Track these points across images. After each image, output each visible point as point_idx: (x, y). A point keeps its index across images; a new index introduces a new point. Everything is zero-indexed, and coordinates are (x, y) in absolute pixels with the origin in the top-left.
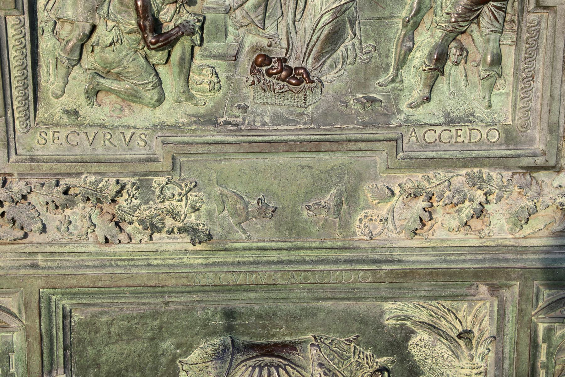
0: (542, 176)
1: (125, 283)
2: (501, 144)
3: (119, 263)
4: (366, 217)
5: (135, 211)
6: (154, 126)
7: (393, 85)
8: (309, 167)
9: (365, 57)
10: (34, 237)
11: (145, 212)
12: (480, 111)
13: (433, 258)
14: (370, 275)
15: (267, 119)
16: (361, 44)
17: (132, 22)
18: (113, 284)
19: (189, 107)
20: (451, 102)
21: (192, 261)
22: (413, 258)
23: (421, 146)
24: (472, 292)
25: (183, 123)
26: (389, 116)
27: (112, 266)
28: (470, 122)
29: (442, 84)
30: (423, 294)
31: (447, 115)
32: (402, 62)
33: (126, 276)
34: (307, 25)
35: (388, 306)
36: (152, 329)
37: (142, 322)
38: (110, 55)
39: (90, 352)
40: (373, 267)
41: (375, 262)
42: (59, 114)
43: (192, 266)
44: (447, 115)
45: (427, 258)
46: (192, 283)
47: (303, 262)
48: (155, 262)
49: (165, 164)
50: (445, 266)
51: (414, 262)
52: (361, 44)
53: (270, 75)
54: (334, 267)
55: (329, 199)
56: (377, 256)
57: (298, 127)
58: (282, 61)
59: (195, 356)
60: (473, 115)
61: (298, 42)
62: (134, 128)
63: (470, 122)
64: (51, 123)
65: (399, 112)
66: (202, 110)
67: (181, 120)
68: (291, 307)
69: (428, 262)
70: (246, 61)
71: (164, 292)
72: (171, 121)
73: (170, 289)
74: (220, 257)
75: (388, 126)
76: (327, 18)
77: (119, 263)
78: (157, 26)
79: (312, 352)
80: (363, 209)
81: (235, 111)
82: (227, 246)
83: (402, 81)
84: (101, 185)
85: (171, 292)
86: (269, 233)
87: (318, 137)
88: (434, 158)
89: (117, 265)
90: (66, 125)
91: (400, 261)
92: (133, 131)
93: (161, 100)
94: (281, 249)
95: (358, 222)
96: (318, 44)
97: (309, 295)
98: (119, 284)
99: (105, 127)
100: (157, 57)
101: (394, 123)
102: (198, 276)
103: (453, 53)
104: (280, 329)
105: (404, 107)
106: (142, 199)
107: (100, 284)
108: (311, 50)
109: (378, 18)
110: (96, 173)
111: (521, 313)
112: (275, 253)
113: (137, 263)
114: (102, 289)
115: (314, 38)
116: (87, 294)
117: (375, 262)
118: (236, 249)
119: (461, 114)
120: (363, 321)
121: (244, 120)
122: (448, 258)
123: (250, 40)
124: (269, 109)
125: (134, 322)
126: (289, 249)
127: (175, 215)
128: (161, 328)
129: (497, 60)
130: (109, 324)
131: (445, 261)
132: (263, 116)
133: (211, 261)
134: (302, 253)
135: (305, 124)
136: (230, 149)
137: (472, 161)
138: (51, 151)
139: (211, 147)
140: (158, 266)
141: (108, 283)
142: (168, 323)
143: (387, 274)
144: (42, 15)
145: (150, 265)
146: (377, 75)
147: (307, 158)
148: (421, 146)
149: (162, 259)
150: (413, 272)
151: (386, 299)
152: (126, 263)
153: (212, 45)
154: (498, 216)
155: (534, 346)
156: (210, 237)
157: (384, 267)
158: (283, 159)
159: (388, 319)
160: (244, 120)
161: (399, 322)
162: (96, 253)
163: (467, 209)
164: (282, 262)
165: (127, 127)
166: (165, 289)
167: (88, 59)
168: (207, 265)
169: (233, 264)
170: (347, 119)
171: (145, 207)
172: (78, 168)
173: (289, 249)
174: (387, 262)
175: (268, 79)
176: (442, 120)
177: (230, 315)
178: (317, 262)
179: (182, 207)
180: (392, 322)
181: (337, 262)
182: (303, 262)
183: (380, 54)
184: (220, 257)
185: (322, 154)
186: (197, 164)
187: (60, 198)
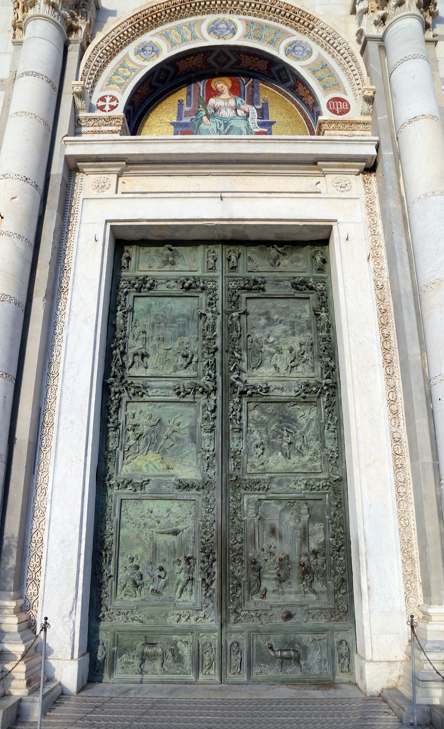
0: (199, 612)
10: (114, 621)
11: (132, 616)
12: (189, 600)
17: (131, 583)
19: (140, 598)
26: (173, 600)
29: (183, 595)
32: (176, 591)
34: (160, 584)
35: (173, 636)
38: (128, 588)
39: (121, 643)
49: (136, 608)
55: (163, 615)
58: (156, 590)
59: (139, 645)
61: (159, 588)
64: (118, 600)
68: (157, 636)
70: (150, 590)
74: (144, 625)
78: (136, 583)
79: (159, 645)
86: (153, 621)
93: (136, 596)
100: (136, 589)
103: (184, 589)
111: (196, 638)
120: (169, 639)
123: (151, 587)
127: (137, 617)
129: (192, 591)
138: (118, 605)
144: (119, 582)
147: (159, 607)
153: (145, 587)
155: (199, 644)
156: (142, 622)
158: (155, 608)
163: (186, 617)
167: (125, 589)
170: (166, 600)
172: (121, 608)
177: (146, 637)
179: (138, 616)
184: (144, 625)
187: (118, 613)
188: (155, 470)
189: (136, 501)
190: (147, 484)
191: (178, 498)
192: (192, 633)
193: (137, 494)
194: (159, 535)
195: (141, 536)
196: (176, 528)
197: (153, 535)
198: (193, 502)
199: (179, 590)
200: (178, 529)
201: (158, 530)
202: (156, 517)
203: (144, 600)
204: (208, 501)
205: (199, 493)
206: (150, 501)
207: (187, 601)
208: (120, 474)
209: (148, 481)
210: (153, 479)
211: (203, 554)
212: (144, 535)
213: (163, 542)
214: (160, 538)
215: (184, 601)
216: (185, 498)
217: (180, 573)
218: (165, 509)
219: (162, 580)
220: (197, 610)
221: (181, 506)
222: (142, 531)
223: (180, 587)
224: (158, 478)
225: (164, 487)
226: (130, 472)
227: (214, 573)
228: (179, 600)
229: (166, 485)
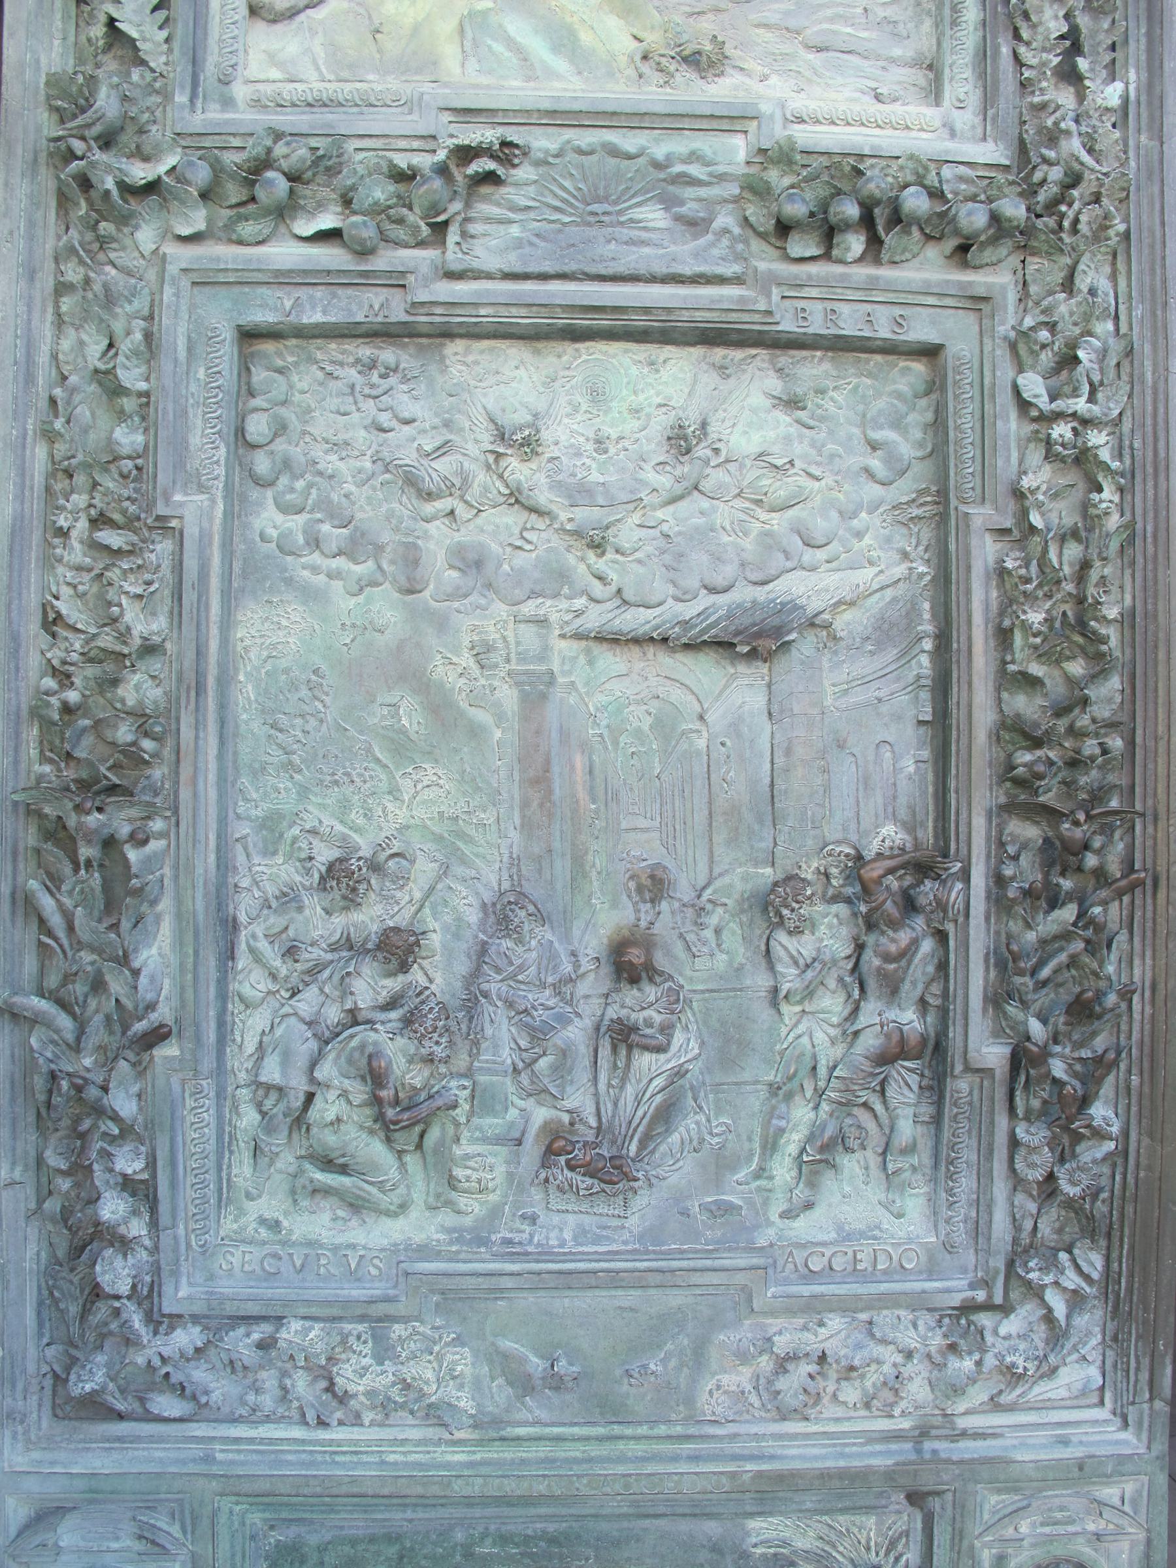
0: (985, 1320)
1: (344, 1489)
2: (921, 1272)
3: (338, 1458)
4: (719, 1387)
5: (362, 1376)
6: (396, 1245)
7: (758, 1183)
8: (632, 1310)
9: (717, 1140)
13: (824, 1451)
14: (724, 1480)
15: (567, 1235)
16: (709, 1121)
18: (327, 1492)
20: (846, 1208)
21: (449, 1457)
22: (794, 1452)
23: (804, 1277)
24: (883, 1502)
25: (438, 1241)
27: (325, 1462)
28: (875, 1238)
30: (809, 1505)
31: (840, 1228)
32: (770, 1145)
33: (347, 1480)
35: (754, 1524)
36: (388, 1559)
37: (373, 1548)
40: (731, 1468)
41: (735, 1458)
42: (254, 1225)
43: (448, 1466)
44: (840, 1228)
45: (815, 1451)
46: (448, 1493)
47: (622, 1459)
48: (392, 1458)
50: (842, 1463)
51: (793, 1458)
52: (709, 1121)
53: (572, 1168)
54: (671, 1469)
56: (736, 1447)
57: (614, 1247)
60: (878, 1227)
62: (364, 1248)
63: (875, 1238)
65: (770, 1224)
66: (468, 1221)
67: (435, 1237)
69: (816, 1458)
71: (405, 1505)
72: (418, 1238)
73: (414, 1501)
75: (751, 1249)
76: (659, 1082)
77: (338, 1458)
80: (714, 1374)
81: (518, 1224)
82: (503, 1433)
83: (771, 1178)
84: (311, 1335)
85: (416, 1505)
87: (646, 1264)
88: (823, 1295)
89: (334, 1462)
90: (264, 1243)
91: (772, 1457)
92: (362, 1253)
94: (587, 1439)
95: (707, 1396)
96: (645, 1121)
97: (631, 1511)
98: (335, 1491)
99: (321, 1246)
101: (762, 1242)
102: (459, 1481)
104: (587, 1559)
105: (774, 1217)
106: (374, 1356)
107: (306, 1491)
108: (635, 1130)
109: (736, 1084)
110: (304, 1318)
112: (579, 1445)
113: (365, 1458)
114: (311, 1500)
115: (640, 1113)
116: (287, 1505)
117: (735, 1458)
118: (518, 1438)
119: (861, 1226)
121: (532, 1236)
122: (847, 1450)
123: (541, 1114)
124: (571, 1218)
125: (360, 1547)
126: (600, 1439)
128: (401, 1557)
130: (322, 1549)
131: (842, 1455)
132: (561, 1230)
133: (478, 1457)
134: (621, 1445)
135: (625, 1243)
136: (508, 1283)
137: (879, 1300)
139: (480, 1280)
140: (395, 1463)
141: (318, 1489)
142: (412, 1549)
143: (753, 1478)
145: (383, 1462)
146: (734, 1169)
148: (804, 1277)
149: (404, 1453)
150: (793, 1475)
151: (752, 1515)
152: (348, 1458)
154: (918, 1381)
157: (749, 1467)
159: (755, 1546)
160: (532, 1236)
161: (772, 1551)
162: (303, 1442)
164: (590, 1460)
165: (353, 1246)
166: (408, 1501)
168: (471, 1465)
169: (512, 1462)
171: (379, 1368)
173: (600, 1439)
174: (752, 1458)
175: (569, 1174)
176: (833, 1235)
178: (645, 1459)
180: (759, 1551)
181: (675, 1458)
182: (622, 1459)
183: (738, 1136)
185: (652, 1291)
186: (460, 1304)
188: (561, 65)
189: (388, 355)
190: (491, 178)
191: (788, 325)
192: (915, 1498)
193: (397, 281)
194: (611, 661)
195: (440, 671)
196: (761, 594)
197: (543, 655)
198: (919, 367)
199: (792, 1143)
200: (793, 607)
201: (594, 619)
202: (579, 493)
203: (478, 1238)
204: (1069, 360)
205: (979, 280)
206: (514, 351)
207: (871, 1233)
208: (228, 102)
209: (507, 152)
210: (542, 141)
211: (1030, 832)
212: (466, 660)
213: (640, 718)
214: (618, 688)
215: (846, 1236)
216: (850, 323)
217: (809, 993)
218: (661, 423)
219: (644, 1061)
220: (968, 1308)
221: (792, 403)
222: (442, 624)
223: (802, 1114)
224: (587, 138)
225: (654, 216)
226: (314, 84)
227: (1126, 995)
228: (801, 1227)
229: (669, 202)
